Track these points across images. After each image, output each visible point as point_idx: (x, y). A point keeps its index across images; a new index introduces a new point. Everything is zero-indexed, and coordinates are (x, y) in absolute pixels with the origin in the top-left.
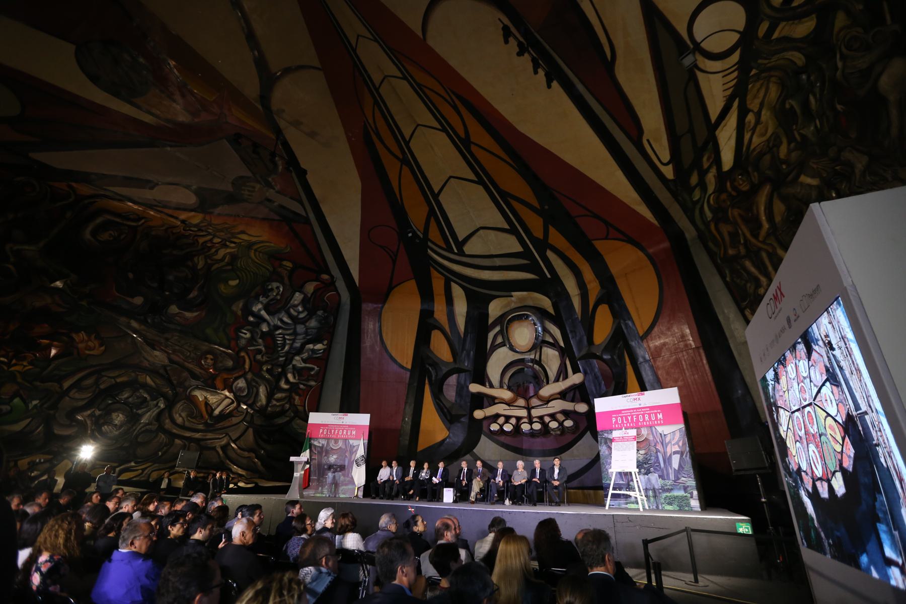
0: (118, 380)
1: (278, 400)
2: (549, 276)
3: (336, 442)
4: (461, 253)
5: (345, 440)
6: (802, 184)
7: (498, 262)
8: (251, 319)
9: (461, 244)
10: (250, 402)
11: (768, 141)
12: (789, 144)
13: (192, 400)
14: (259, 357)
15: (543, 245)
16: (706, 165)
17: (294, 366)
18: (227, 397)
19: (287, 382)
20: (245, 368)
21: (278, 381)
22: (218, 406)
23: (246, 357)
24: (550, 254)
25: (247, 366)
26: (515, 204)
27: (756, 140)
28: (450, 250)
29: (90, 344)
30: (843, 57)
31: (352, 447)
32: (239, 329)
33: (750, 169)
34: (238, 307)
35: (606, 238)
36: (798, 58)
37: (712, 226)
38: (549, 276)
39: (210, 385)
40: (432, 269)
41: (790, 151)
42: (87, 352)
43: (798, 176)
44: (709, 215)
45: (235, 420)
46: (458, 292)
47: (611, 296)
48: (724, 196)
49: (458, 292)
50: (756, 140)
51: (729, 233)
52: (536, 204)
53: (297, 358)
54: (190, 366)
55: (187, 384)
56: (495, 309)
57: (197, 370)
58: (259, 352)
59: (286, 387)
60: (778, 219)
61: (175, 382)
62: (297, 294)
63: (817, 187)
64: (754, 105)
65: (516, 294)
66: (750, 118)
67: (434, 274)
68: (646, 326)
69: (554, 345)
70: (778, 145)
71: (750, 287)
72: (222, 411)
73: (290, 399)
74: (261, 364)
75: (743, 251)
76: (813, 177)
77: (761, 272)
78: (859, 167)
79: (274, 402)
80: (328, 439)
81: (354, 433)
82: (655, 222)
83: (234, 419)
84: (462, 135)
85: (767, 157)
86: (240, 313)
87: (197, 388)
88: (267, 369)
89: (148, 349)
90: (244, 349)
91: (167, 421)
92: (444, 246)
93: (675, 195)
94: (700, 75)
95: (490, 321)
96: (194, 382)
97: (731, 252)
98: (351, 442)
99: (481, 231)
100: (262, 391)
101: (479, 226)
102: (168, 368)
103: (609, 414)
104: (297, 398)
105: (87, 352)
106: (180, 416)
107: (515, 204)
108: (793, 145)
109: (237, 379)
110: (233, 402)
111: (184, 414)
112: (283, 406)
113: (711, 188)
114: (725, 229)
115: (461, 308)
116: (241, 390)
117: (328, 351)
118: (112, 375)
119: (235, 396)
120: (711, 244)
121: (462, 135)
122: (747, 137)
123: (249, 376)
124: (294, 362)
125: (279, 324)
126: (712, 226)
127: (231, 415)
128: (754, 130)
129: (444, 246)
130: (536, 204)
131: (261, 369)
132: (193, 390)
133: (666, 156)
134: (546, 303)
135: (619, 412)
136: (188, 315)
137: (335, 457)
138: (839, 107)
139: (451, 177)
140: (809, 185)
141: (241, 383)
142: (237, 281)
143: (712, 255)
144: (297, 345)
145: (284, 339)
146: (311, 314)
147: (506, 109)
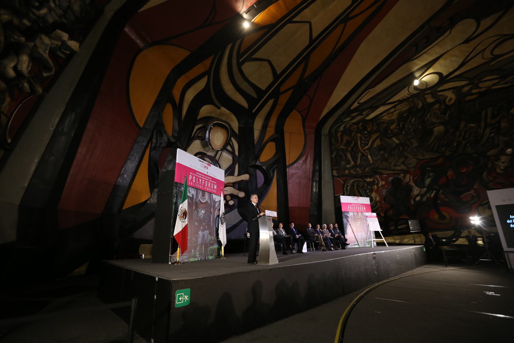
2: (253, 111)
3: (203, 195)
4: (240, 65)
5: (210, 193)
6: (392, 140)
7: (244, 86)
9: (250, 59)
11: (390, 120)
12: (396, 126)
15: (276, 95)
16: (364, 113)
17: (35, 46)
24: (271, 102)
26: (302, 67)
27: (386, 117)
28: (239, 56)
30: (430, 115)
31: (215, 202)
33: (375, 125)
35: (300, 113)
36: (420, 105)
37: (339, 134)
38: (253, 111)
40: (211, 58)
41: (395, 128)
43: (393, 137)
44: (342, 128)
46: (201, 85)
47: (279, 140)
48: (355, 126)
49: (201, 85)
50: (386, 117)
51: (347, 141)
52: (306, 75)
56: (205, 110)
60: (375, 145)
63: (397, 144)
64: (397, 108)
65: (223, 109)
66: (393, 110)
67: (207, 62)
68: (291, 162)
69: (232, 153)
70: (392, 123)
71: (343, 163)
75: (349, 149)
76: (398, 140)
77: (353, 160)
78: (414, 145)
80: (197, 189)
81: (215, 187)
82: (321, 118)
84: (350, 16)
85: (385, 125)
92: (241, 51)
93: (343, 114)
94: (407, 88)
95: (199, 118)
97: (342, 147)
98: (214, 196)
99: (266, 63)
101: (269, 59)
103: (347, 204)
104: (8, 99)
107: (302, 67)
108: (397, 127)
113: (354, 121)
114: (346, 138)
115: (190, 95)
120: (333, 140)
121: (350, 16)
122: (384, 114)
126: (339, 134)
128: (389, 114)
129: (241, 51)
130: (306, 75)
133: (362, 101)
134: (235, 125)
135: (351, 204)
137: (203, 212)
138: (420, 127)
139: (310, 23)
140: (395, 142)
143: (331, 144)
147: (377, 30)
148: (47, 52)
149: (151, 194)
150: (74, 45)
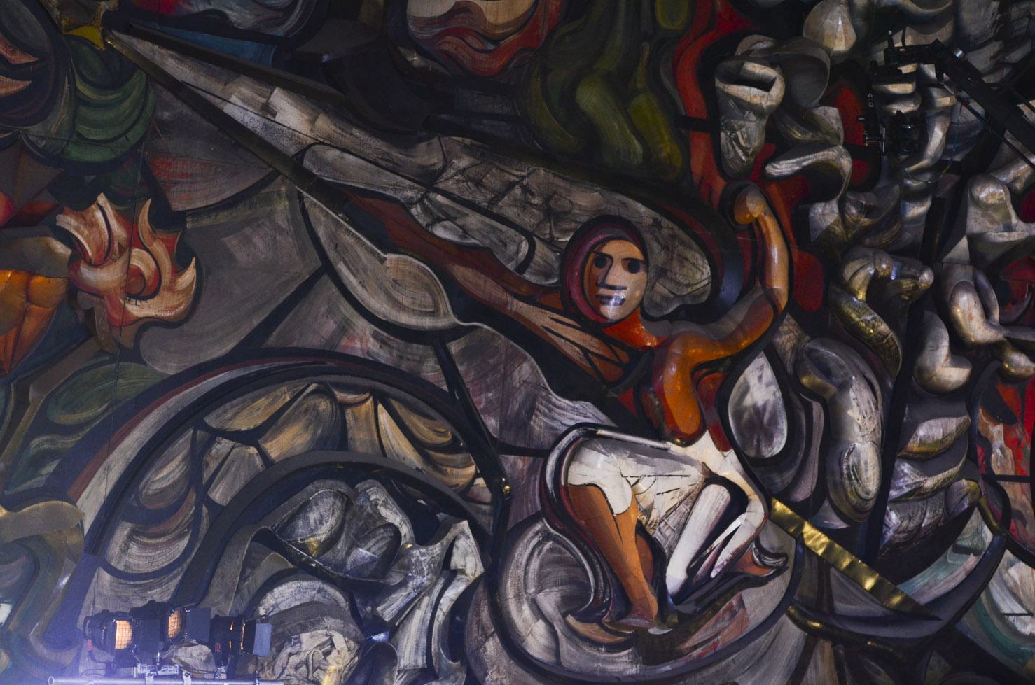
0: (276, 447)
1: (926, 460)
10: (804, 492)
13: (576, 514)
14: (826, 214)
17: (974, 240)
18: (712, 478)
20: (770, 296)
21: (915, 342)
22: (681, 528)
23: (771, 226)
29: (140, 260)
32: (718, 60)
39: (640, 420)
42: (138, 310)
45: (758, 603)
53: (989, 193)
54: (542, 318)
55: (539, 424)
57: (571, 338)
58: (816, 184)
59: (954, 375)
61: (492, 423)
72: (699, 557)
73: (970, 446)
79: (908, 475)
83: (751, 597)
87: (588, 436)
88: (877, 285)
89: (357, 243)
90: (755, 174)
91: (492, 647)
100: (861, 414)
102: (454, 348)
104: (997, 432)
105: (138, 310)
106: (539, 613)
110: (738, 504)
111: (549, 601)
112: (945, 489)
116: (758, 424)
118: (244, 423)
119: (750, 466)
123: (787, 338)
124: (976, 222)
127: (737, 577)
132: (574, 452)
141: (759, 387)
148: (1014, 220)
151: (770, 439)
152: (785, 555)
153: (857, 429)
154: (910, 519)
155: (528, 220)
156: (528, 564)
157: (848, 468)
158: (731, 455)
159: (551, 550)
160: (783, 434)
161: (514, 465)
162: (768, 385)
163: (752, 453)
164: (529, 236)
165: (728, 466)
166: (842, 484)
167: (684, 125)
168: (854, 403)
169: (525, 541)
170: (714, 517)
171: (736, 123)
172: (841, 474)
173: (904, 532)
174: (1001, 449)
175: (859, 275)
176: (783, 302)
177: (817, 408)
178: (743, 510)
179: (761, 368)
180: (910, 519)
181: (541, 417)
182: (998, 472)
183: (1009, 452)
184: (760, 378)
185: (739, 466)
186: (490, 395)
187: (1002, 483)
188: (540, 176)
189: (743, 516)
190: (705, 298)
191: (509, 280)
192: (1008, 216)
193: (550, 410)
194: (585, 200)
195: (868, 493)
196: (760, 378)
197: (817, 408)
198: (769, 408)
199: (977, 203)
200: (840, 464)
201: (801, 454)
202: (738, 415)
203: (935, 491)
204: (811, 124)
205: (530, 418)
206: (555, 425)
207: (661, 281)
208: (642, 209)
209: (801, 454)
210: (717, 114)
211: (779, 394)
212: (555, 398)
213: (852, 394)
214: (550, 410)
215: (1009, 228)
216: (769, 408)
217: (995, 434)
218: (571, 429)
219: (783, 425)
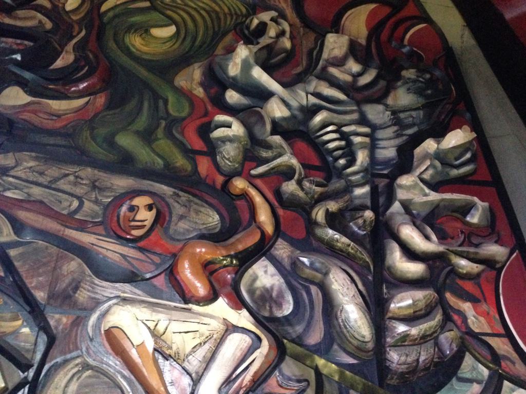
8: (232, 97)
14: (290, 187)
18: (231, 329)
19: (410, 254)
21: (379, 255)
25: (264, 217)
34: (192, 78)
53: (405, 180)
54: (86, 239)
55: (82, 296)
61: (40, 296)
62: (331, 38)
74: (303, 209)
86: (200, 92)
88: (328, 214)
96: (107, 289)
109: (246, 259)
116: (266, 298)
117: (482, 148)
119: (259, 320)
123: (282, 250)
124: (401, 194)
125: (313, 100)
131: (311, 224)
136: (56, 105)
141: (264, 275)
142: (172, 29)
144: (388, 151)
145: (344, 136)
146: (390, 76)
148: (427, 191)
149: (355, 347)
150: (456, 138)
151: (280, 306)
152: (306, 380)
153: (341, 296)
154: (407, 356)
155: (79, 191)
156: (66, 386)
157: (343, 321)
158: (245, 312)
159: (90, 377)
160: (290, 304)
161: (58, 321)
162: (272, 276)
163: (267, 314)
164: (79, 198)
165: (243, 319)
166: (342, 332)
167: (190, 154)
168: (333, 280)
169: (65, 370)
170: (239, 354)
171: (221, 149)
172: (340, 328)
173: (404, 364)
174: (474, 317)
175: (319, 214)
176: (269, 229)
177: (314, 289)
178: (259, 348)
179: (266, 266)
180: (407, 356)
181: (85, 292)
182: (477, 331)
183: (482, 319)
184: (266, 272)
185: (251, 319)
186: (41, 279)
187: (483, 337)
188: (88, 172)
189: (259, 351)
190: (217, 230)
191: (69, 220)
192: (422, 190)
193: (93, 288)
194: (122, 183)
195: (364, 337)
196: (266, 272)
197: (314, 289)
198: (276, 289)
199: (401, 186)
200: (337, 319)
201: (307, 314)
202: (251, 292)
203: (424, 339)
204: (268, 147)
205: (75, 293)
206: (97, 296)
207: (183, 221)
208: (165, 188)
209: (307, 314)
210: (212, 149)
211: (282, 280)
212: (97, 281)
213: (331, 276)
214: (93, 288)
215: (426, 195)
216: (276, 289)
217: (466, 308)
218: (110, 299)
219: (289, 298)
